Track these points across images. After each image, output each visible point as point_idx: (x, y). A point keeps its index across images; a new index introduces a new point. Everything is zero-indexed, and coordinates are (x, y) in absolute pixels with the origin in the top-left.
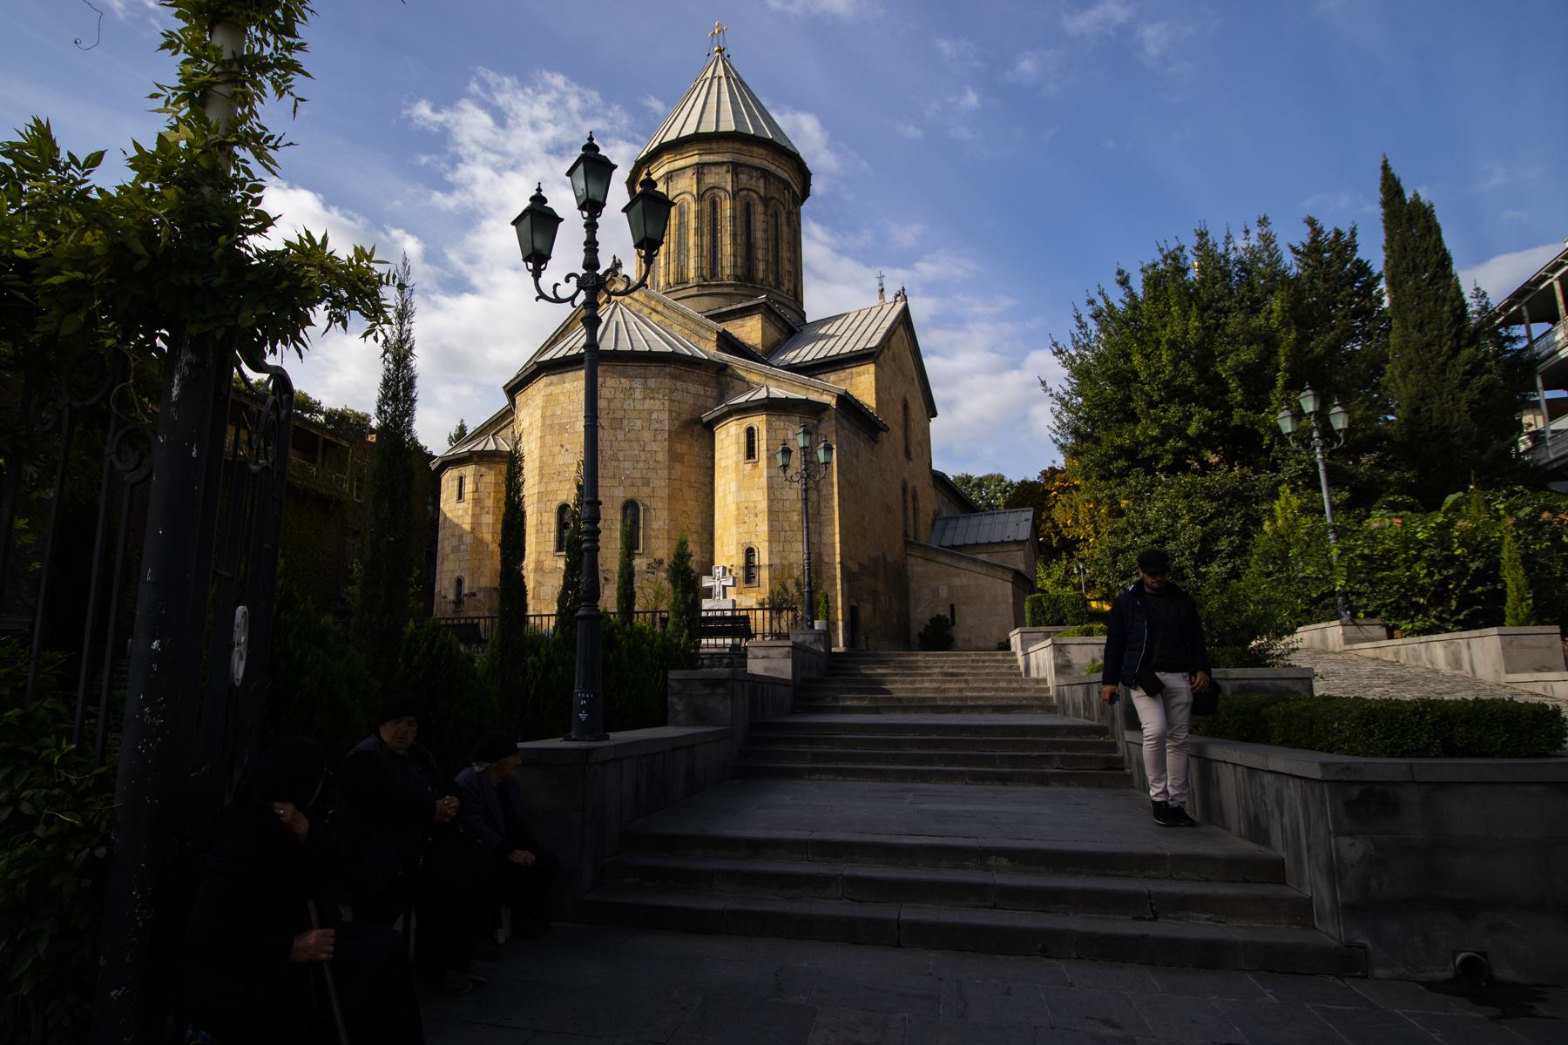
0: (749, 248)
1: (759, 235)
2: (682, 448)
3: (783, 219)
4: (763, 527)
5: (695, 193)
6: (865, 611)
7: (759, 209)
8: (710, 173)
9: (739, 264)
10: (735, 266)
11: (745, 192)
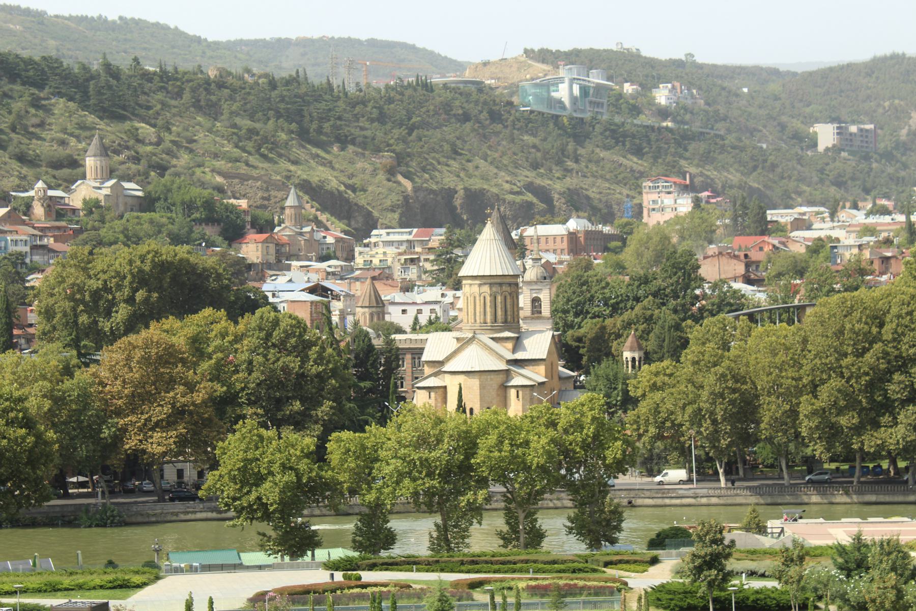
0: (506, 311)
1: (508, 307)
7: (508, 297)
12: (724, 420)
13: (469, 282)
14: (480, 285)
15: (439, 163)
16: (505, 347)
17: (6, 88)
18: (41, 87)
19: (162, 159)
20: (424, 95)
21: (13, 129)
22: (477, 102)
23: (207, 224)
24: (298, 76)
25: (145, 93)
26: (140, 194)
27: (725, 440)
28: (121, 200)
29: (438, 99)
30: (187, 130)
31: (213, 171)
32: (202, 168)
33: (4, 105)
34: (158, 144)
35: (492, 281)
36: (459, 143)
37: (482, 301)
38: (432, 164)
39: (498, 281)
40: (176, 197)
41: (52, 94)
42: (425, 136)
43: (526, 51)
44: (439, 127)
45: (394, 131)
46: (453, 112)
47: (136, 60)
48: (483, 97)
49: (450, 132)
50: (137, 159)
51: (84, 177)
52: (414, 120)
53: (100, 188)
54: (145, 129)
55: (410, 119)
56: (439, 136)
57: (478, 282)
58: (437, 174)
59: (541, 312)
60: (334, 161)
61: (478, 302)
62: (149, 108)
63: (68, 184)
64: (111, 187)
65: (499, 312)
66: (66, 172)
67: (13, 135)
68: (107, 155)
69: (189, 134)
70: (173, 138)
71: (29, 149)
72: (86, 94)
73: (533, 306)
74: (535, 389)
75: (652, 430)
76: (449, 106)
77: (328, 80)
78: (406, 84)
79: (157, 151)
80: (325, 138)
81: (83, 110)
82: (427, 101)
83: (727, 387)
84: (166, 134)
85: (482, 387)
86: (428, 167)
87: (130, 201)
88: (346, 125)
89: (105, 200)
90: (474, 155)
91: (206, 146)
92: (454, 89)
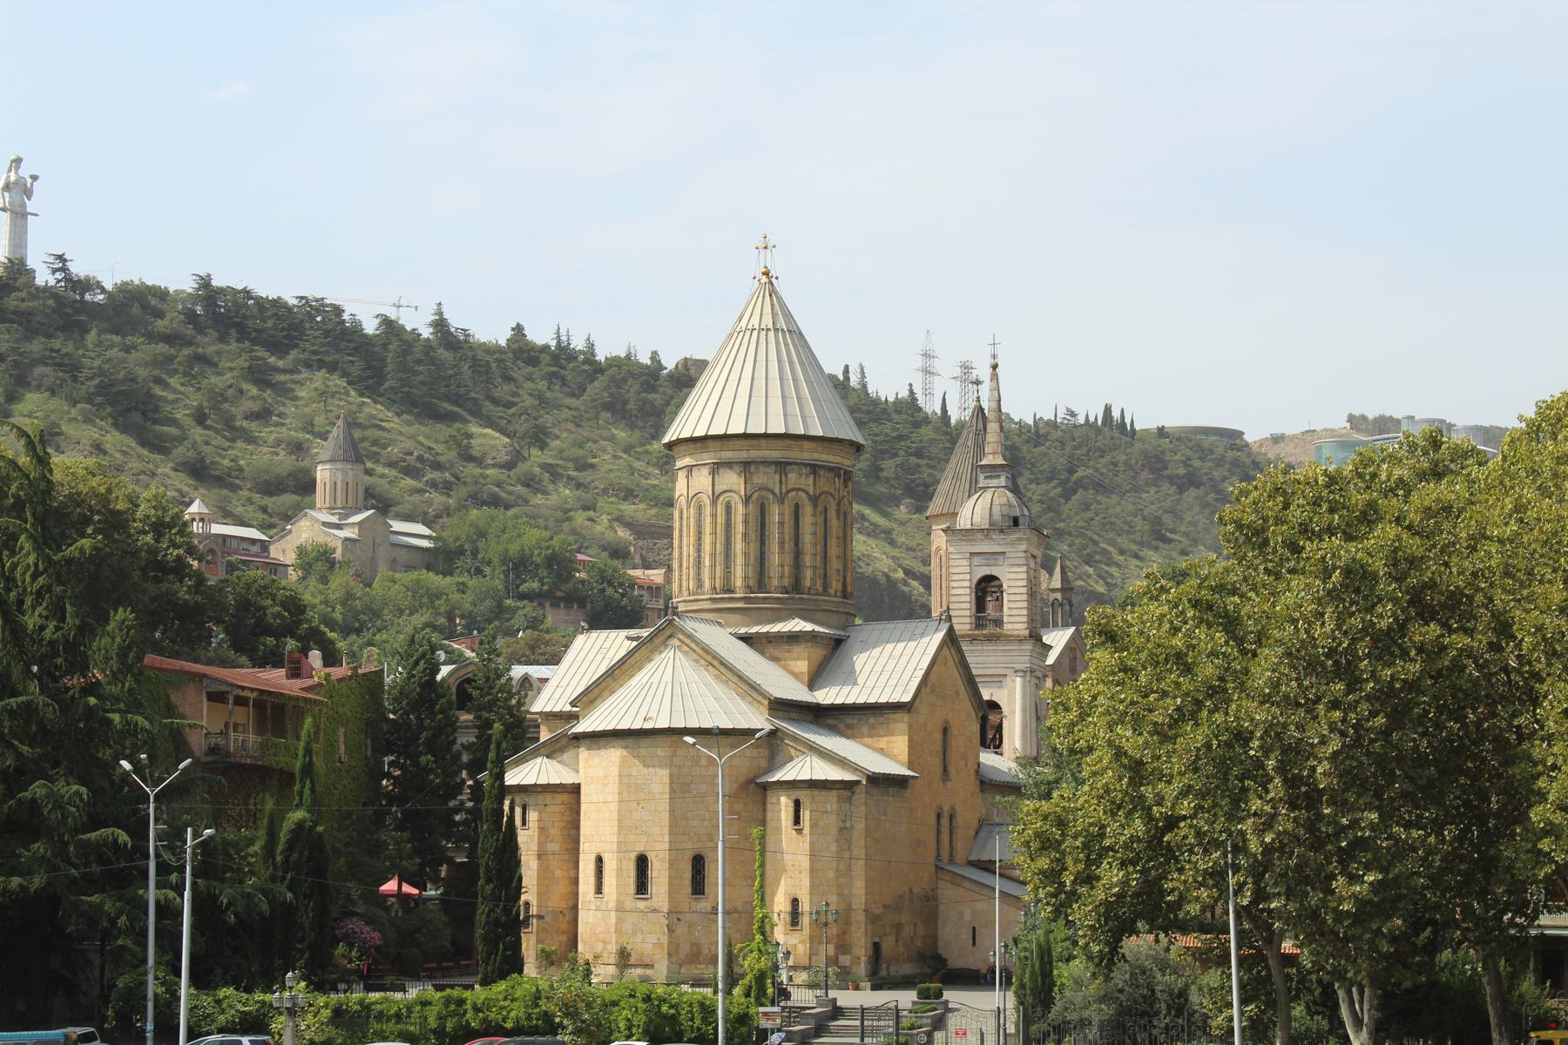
0: (798, 554)
1: (807, 539)
2: (738, 807)
3: (832, 513)
4: (806, 882)
5: (743, 493)
6: (888, 945)
7: (807, 509)
8: (758, 471)
9: (786, 574)
10: (782, 577)
11: (794, 493)
12: (1350, 778)
13: (687, 461)
14: (716, 468)
15: (1122, 552)
16: (784, 667)
17: (210, 350)
18: (278, 348)
19: (511, 493)
20: (1112, 438)
21: (200, 418)
22: (1220, 462)
23: (555, 605)
24: (847, 378)
25: (508, 379)
26: (425, 543)
27: (1353, 879)
28: (382, 553)
29: (1138, 446)
30: (581, 445)
31: (617, 519)
32: (591, 513)
33: (194, 377)
34: (509, 466)
35: (754, 454)
36: (1168, 520)
37: (721, 520)
38: (1105, 552)
39: (775, 455)
40: (493, 549)
41: (308, 365)
42: (1099, 503)
43: (1351, 419)
44: (1136, 489)
45: (1033, 486)
46: (1169, 472)
47: (519, 329)
48: (1230, 454)
49: (1154, 500)
50: (447, 487)
51: (312, 506)
52: (1080, 473)
53: (338, 527)
54: (488, 439)
55: (1072, 471)
56: (1130, 508)
57: (708, 458)
58: (1114, 570)
59: (998, 622)
60: (897, 529)
61: (708, 521)
62: (509, 405)
63: (277, 522)
64: (360, 524)
65: (775, 557)
66: (289, 499)
67: (197, 433)
68: (359, 460)
69: (580, 452)
70: (549, 461)
71: (223, 457)
72: (380, 376)
73: (980, 605)
74: (860, 796)
75: (1111, 875)
76: (1160, 460)
77: (911, 392)
78: (1081, 420)
79: (503, 477)
80: (881, 489)
81: (362, 395)
82: (1115, 448)
83: (1368, 629)
84: (535, 451)
85: (679, 788)
86: (1098, 557)
87: (402, 555)
88: (931, 467)
89: (345, 549)
90: (1195, 541)
91: (612, 476)
92: (1179, 439)
